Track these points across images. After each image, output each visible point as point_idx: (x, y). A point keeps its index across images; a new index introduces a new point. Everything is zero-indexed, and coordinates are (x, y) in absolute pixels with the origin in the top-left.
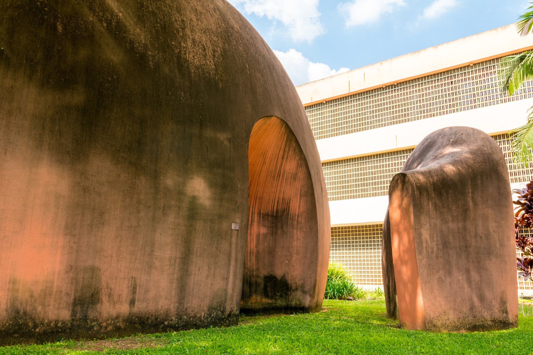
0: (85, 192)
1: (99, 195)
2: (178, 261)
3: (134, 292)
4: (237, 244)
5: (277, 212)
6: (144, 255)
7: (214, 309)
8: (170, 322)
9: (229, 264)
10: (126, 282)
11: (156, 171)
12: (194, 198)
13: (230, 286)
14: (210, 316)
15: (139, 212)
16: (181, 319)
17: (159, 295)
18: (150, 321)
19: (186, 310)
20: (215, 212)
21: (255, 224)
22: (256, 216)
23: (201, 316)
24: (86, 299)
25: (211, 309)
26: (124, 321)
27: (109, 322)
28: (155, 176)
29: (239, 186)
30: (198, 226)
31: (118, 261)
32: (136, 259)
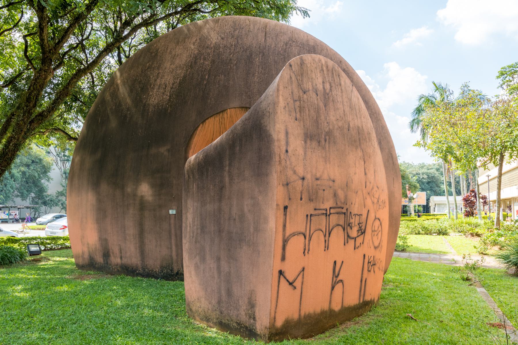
2: (137, 236)
25: (162, 267)
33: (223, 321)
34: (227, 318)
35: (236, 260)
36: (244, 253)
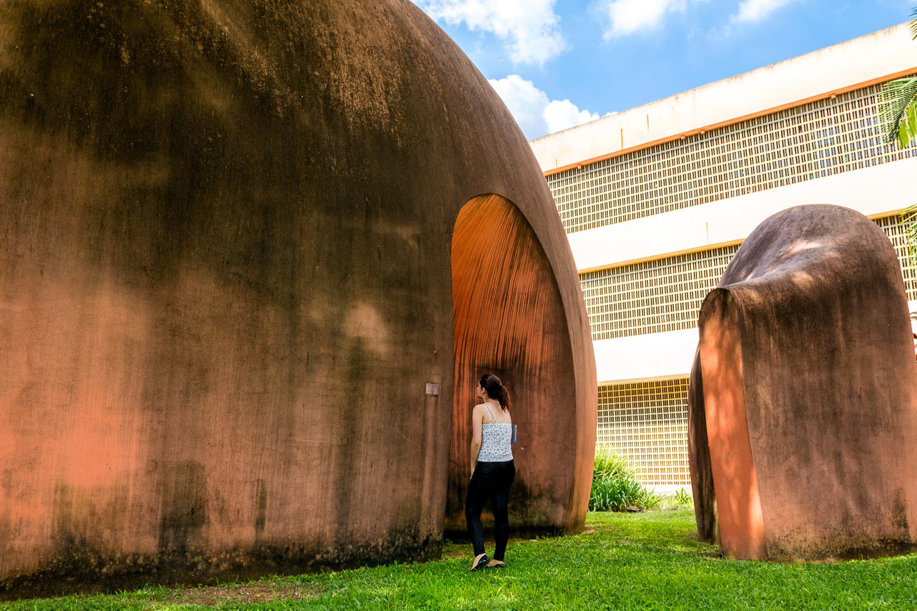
0: (174, 335)
1: (198, 339)
2: (335, 451)
3: (262, 506)
4: (436, 420)
5: (503, 361)
6: (277, 442)
7: (400, 532)
8: (325, 556)
9: (423, 455)
10: (248, 487)
11: (292, 296)
12: (359, 342)
13: (426, 492)
14: (394, 544)
15: (265, 367)
16: (343, 550)
17: (306, 507)
18: (290, 554)
19: (352, 535)
20: (396, 365)
21: (466, 384)
22: (466, 369)
23: (377, 544)
24: (183, 517)
25: (394, 532)
26: (248, 554)
27: (222, 556)
28: (292, 304)
29: (436, 318)
30: (367, 390)
31: (233, 452)
32: (263, 449)
33: (855, 546)
34: (861, 539)
35: (870, 453)
36: (879, 443)
